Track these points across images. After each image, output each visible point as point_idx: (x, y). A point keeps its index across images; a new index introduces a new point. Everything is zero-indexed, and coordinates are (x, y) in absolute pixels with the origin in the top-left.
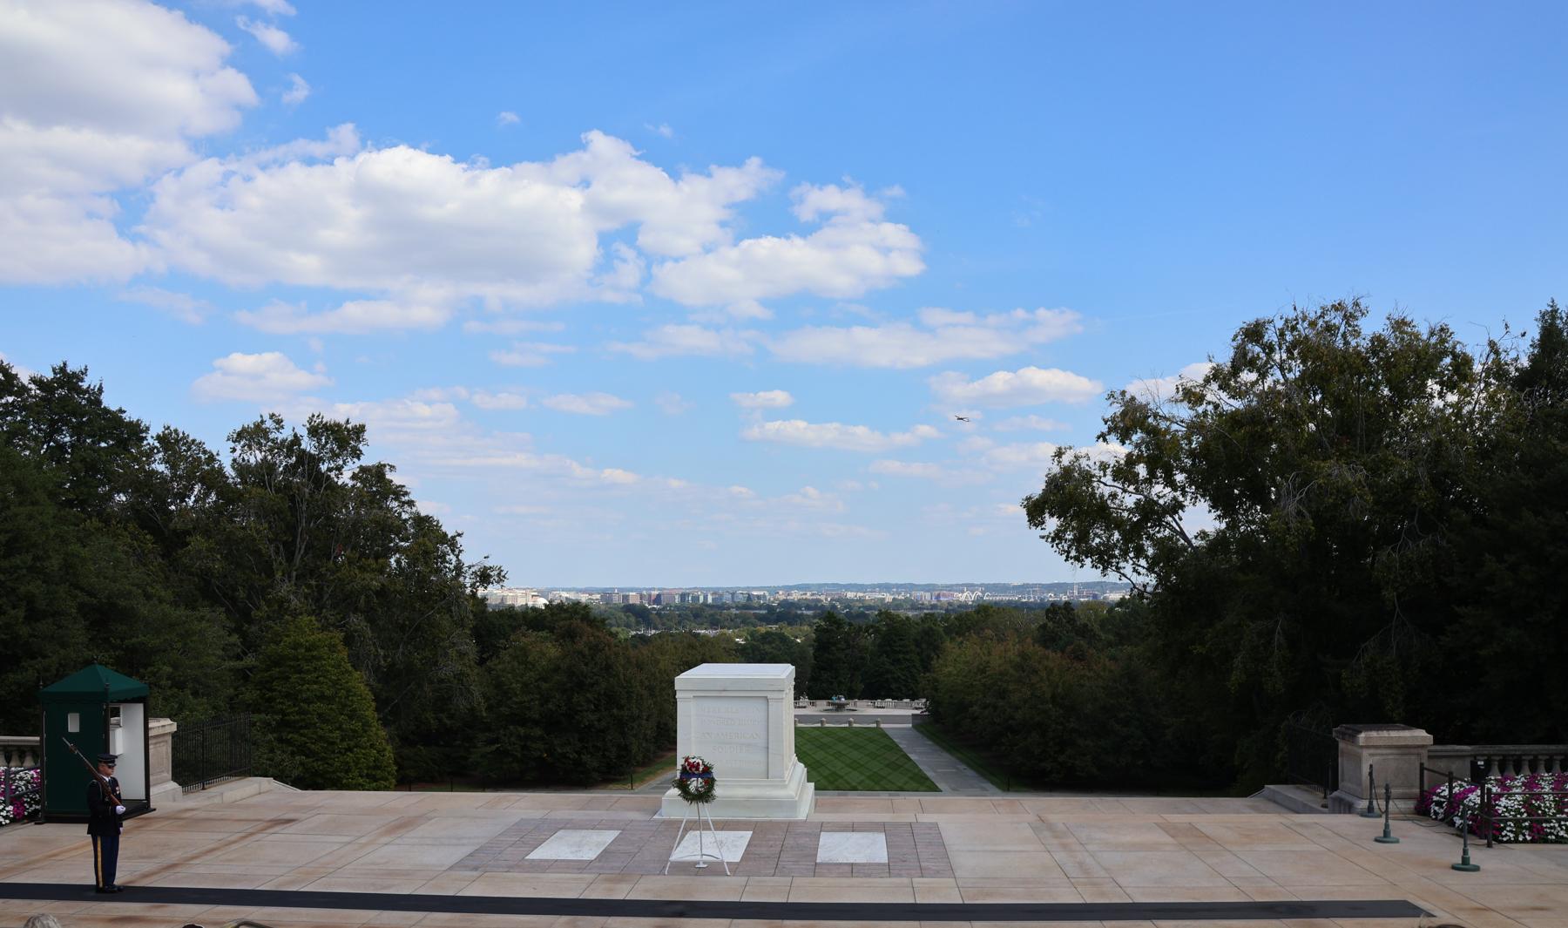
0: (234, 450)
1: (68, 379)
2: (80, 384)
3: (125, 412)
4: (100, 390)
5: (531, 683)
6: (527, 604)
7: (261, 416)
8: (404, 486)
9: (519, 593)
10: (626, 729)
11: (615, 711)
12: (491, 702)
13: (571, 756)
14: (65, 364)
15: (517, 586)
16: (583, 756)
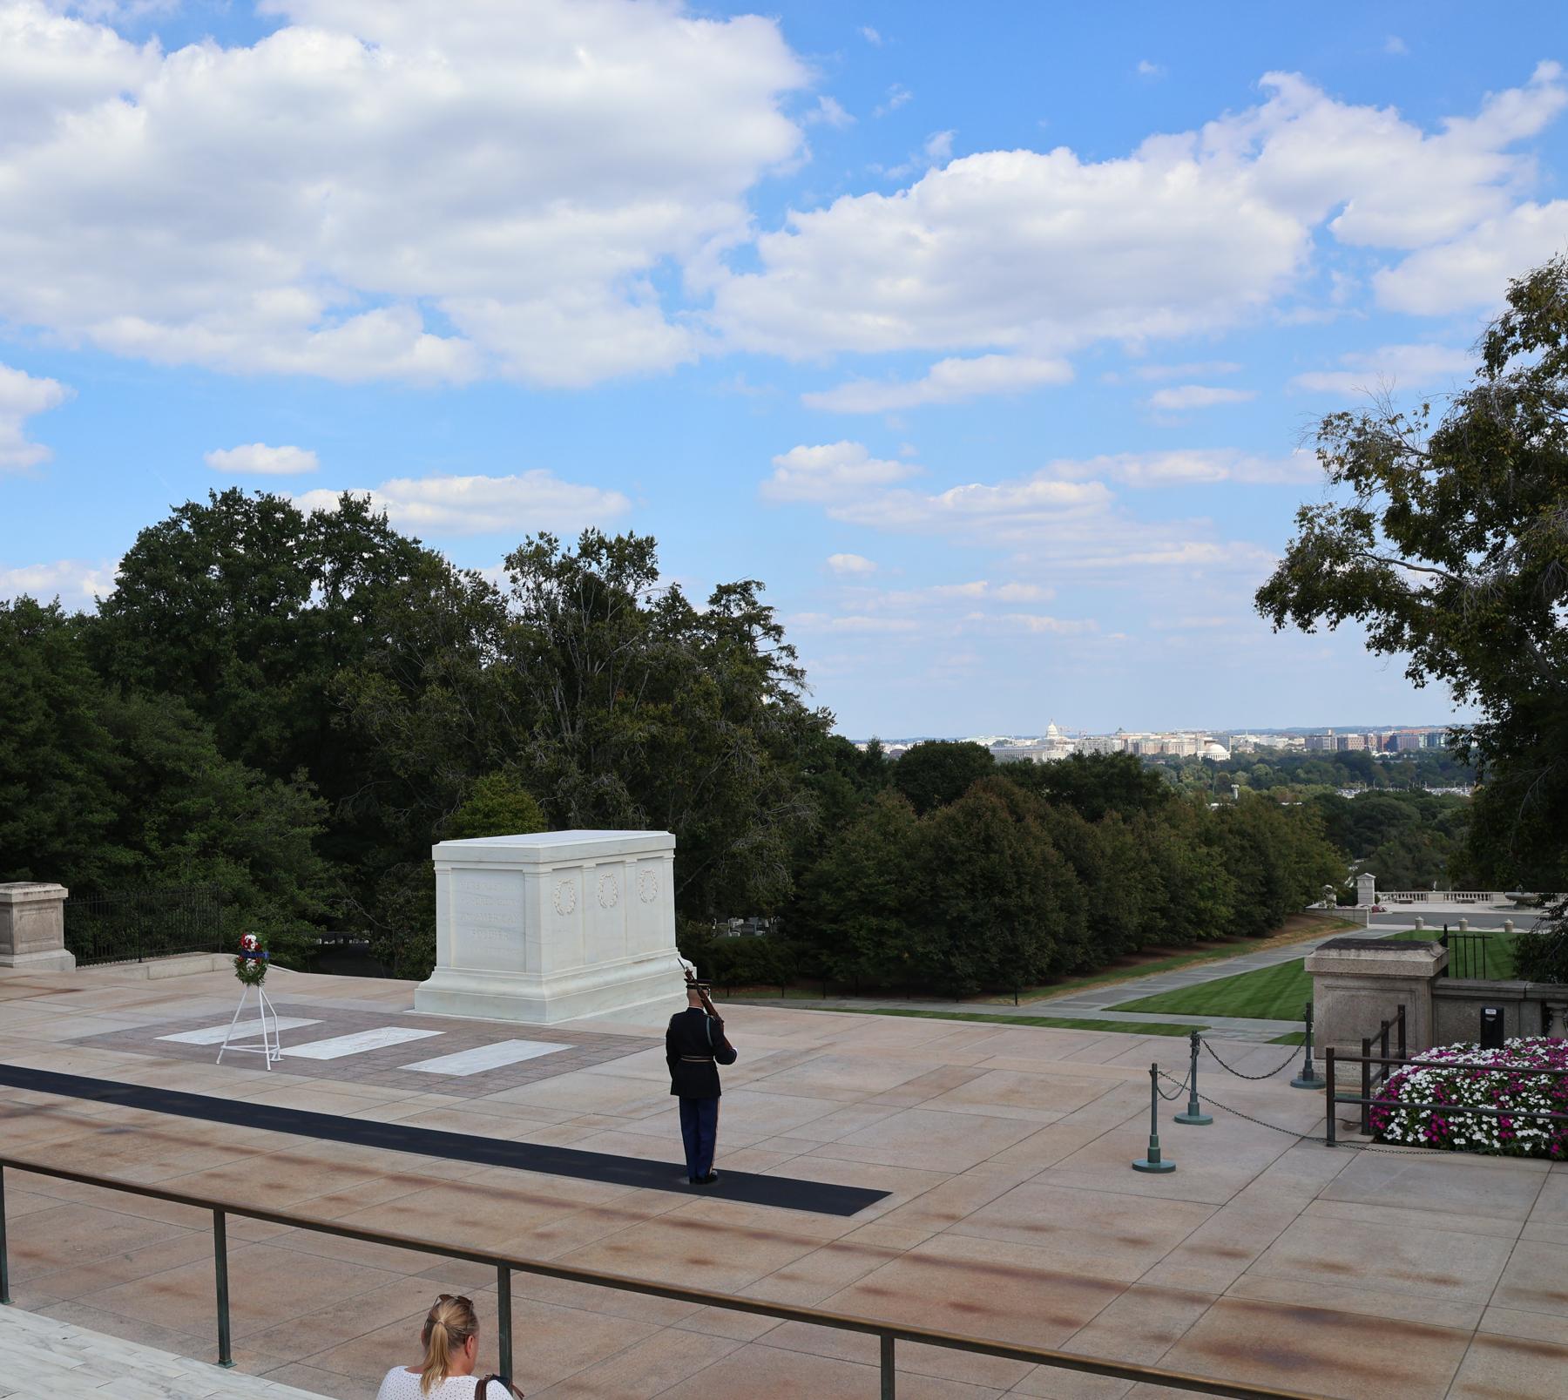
0: (514, 580)
1: (352, 510)
2: (364, 514)
3: (420, 542)
4: (385, 519)
5: (890, 860)
6: (1195, 754)
7: (528, 537)
8: (771, 608)
9: (1186, 739)
10: (1016, 924)
11: (996, 899)
12: (838, 883)
13: (936, 958)
14: (346, 494)
15: (1187, 730)
16: (952, 959)
